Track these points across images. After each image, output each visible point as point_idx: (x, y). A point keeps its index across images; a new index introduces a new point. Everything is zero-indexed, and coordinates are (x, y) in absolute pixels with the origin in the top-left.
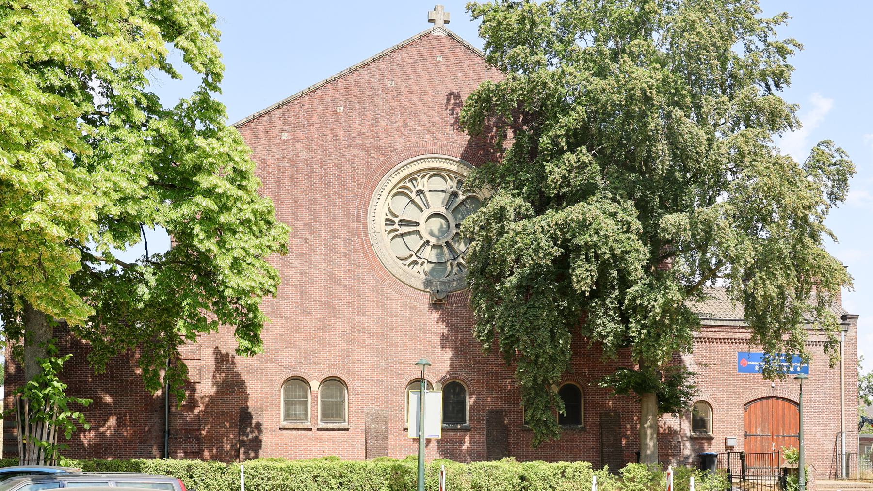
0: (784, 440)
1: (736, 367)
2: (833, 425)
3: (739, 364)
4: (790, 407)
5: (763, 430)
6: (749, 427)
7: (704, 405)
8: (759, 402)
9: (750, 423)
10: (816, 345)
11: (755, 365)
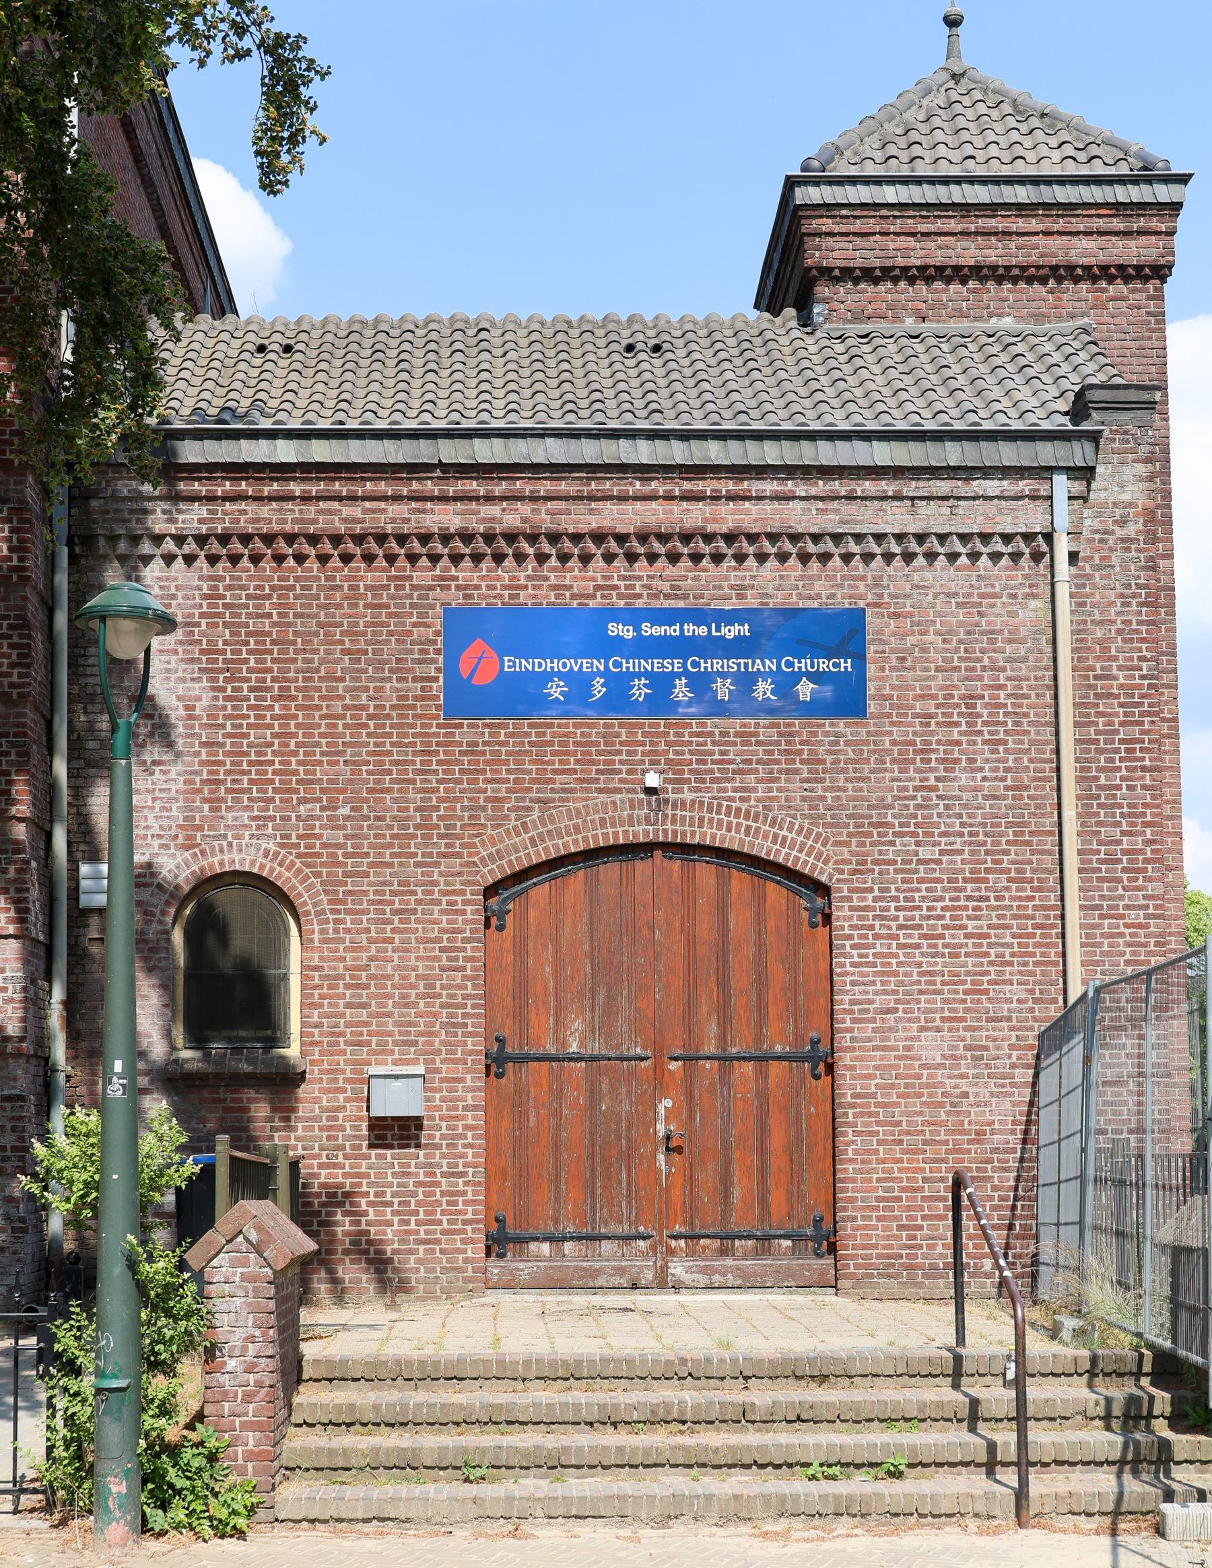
0: (725, 1077)
1: (437, 687)
2: (1015, 992)
3: (450, 670)
4: (760, 899)
5: (604, 1024)
6: (521, 1013)
7: (254, 895)
8: (578, 879)
9: (522, 986)
10: (909, 557)
11: (548, 676)
